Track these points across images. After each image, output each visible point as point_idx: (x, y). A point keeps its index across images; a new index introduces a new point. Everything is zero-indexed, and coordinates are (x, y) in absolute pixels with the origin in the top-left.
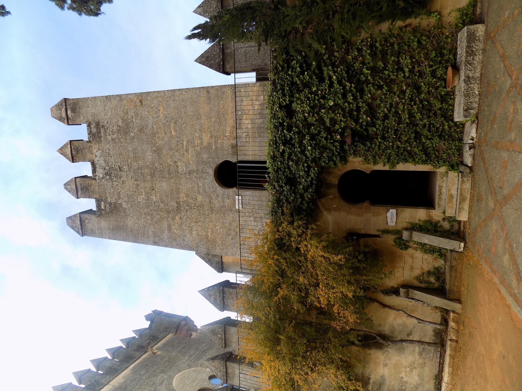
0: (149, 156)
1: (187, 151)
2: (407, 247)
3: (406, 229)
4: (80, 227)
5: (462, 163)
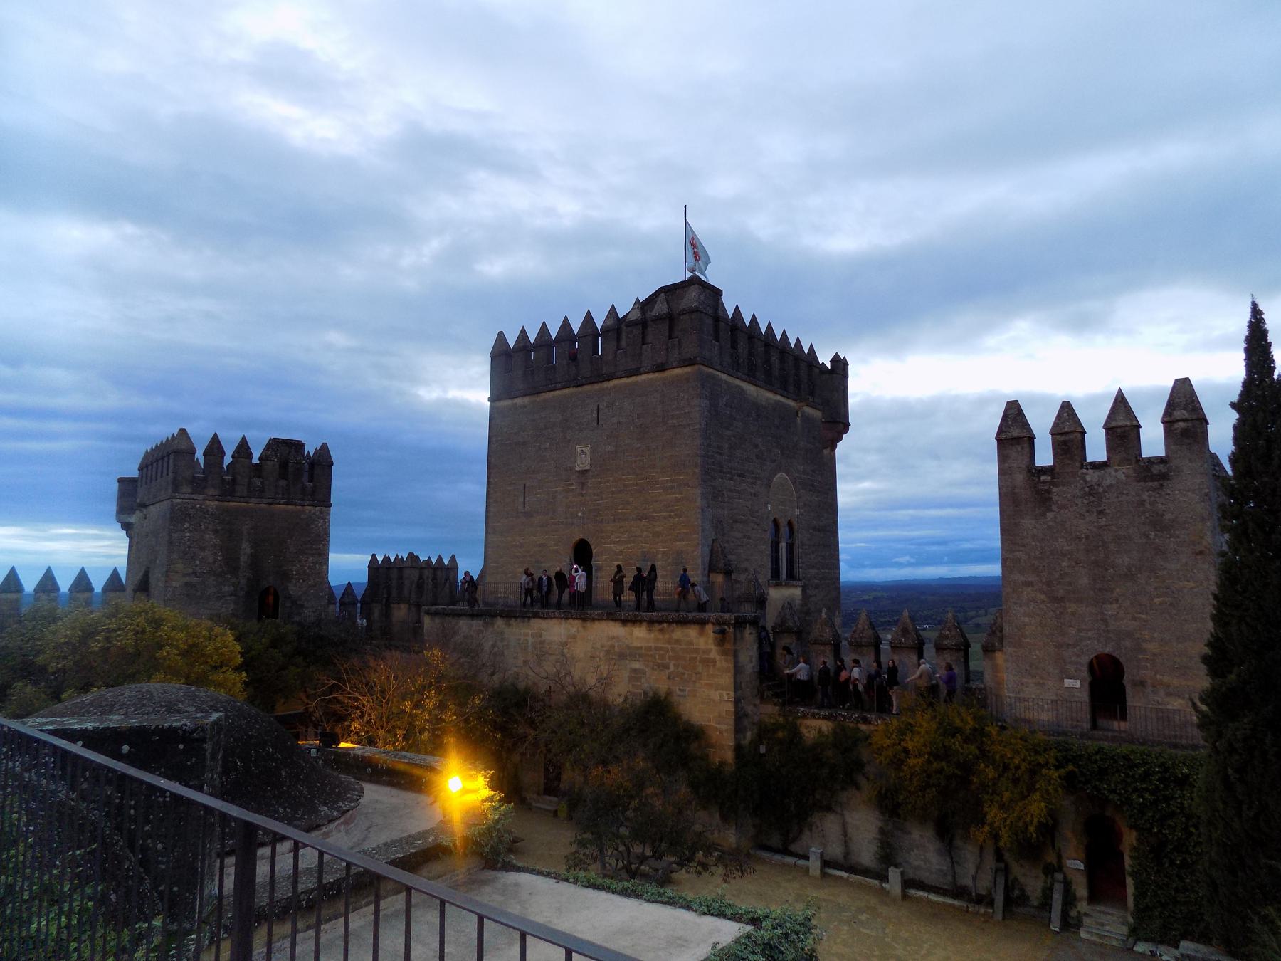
0: (1123, 561)
1: (1134, 619)
2: (1046, 874)
3: (1065, 877)
4: (1009, 435)
5: (1138, 939)
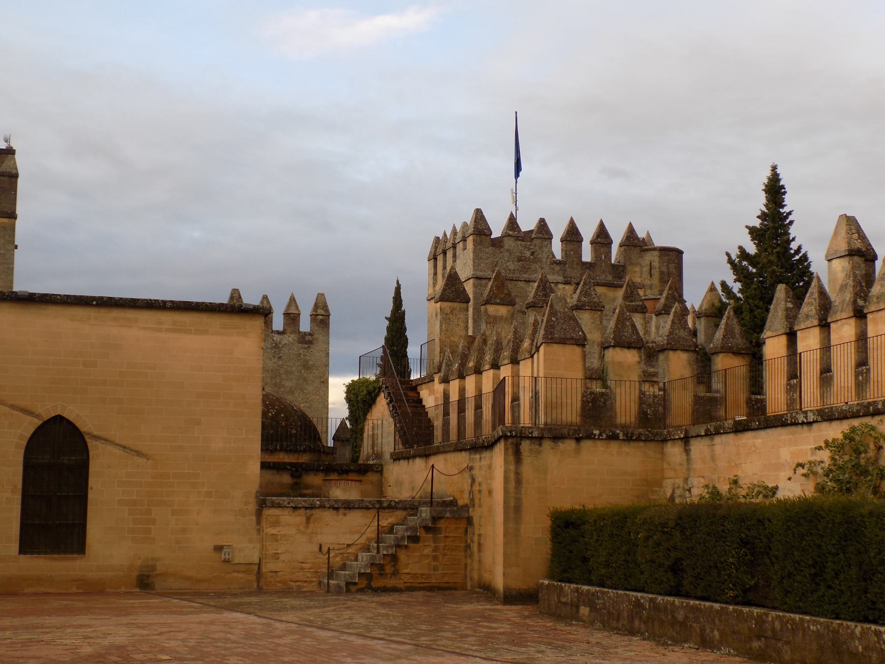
0: (288, 384)
